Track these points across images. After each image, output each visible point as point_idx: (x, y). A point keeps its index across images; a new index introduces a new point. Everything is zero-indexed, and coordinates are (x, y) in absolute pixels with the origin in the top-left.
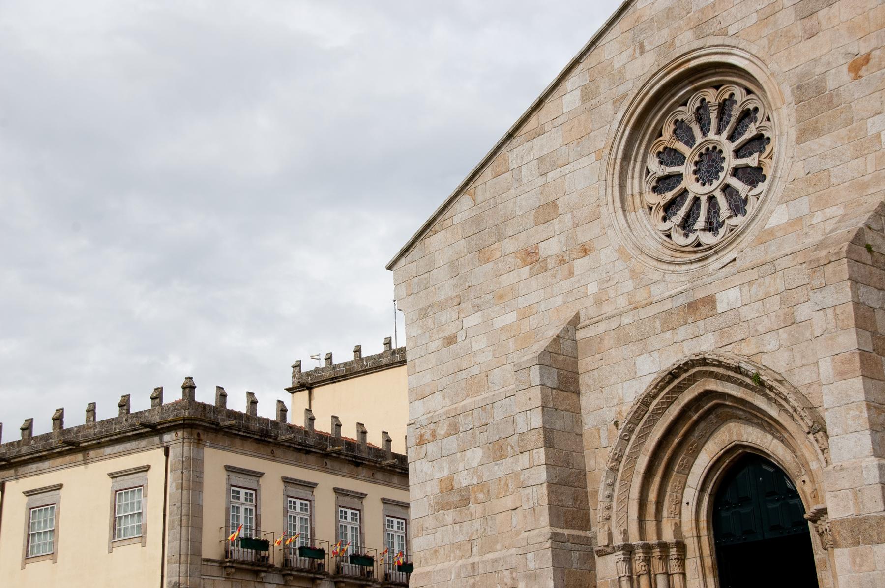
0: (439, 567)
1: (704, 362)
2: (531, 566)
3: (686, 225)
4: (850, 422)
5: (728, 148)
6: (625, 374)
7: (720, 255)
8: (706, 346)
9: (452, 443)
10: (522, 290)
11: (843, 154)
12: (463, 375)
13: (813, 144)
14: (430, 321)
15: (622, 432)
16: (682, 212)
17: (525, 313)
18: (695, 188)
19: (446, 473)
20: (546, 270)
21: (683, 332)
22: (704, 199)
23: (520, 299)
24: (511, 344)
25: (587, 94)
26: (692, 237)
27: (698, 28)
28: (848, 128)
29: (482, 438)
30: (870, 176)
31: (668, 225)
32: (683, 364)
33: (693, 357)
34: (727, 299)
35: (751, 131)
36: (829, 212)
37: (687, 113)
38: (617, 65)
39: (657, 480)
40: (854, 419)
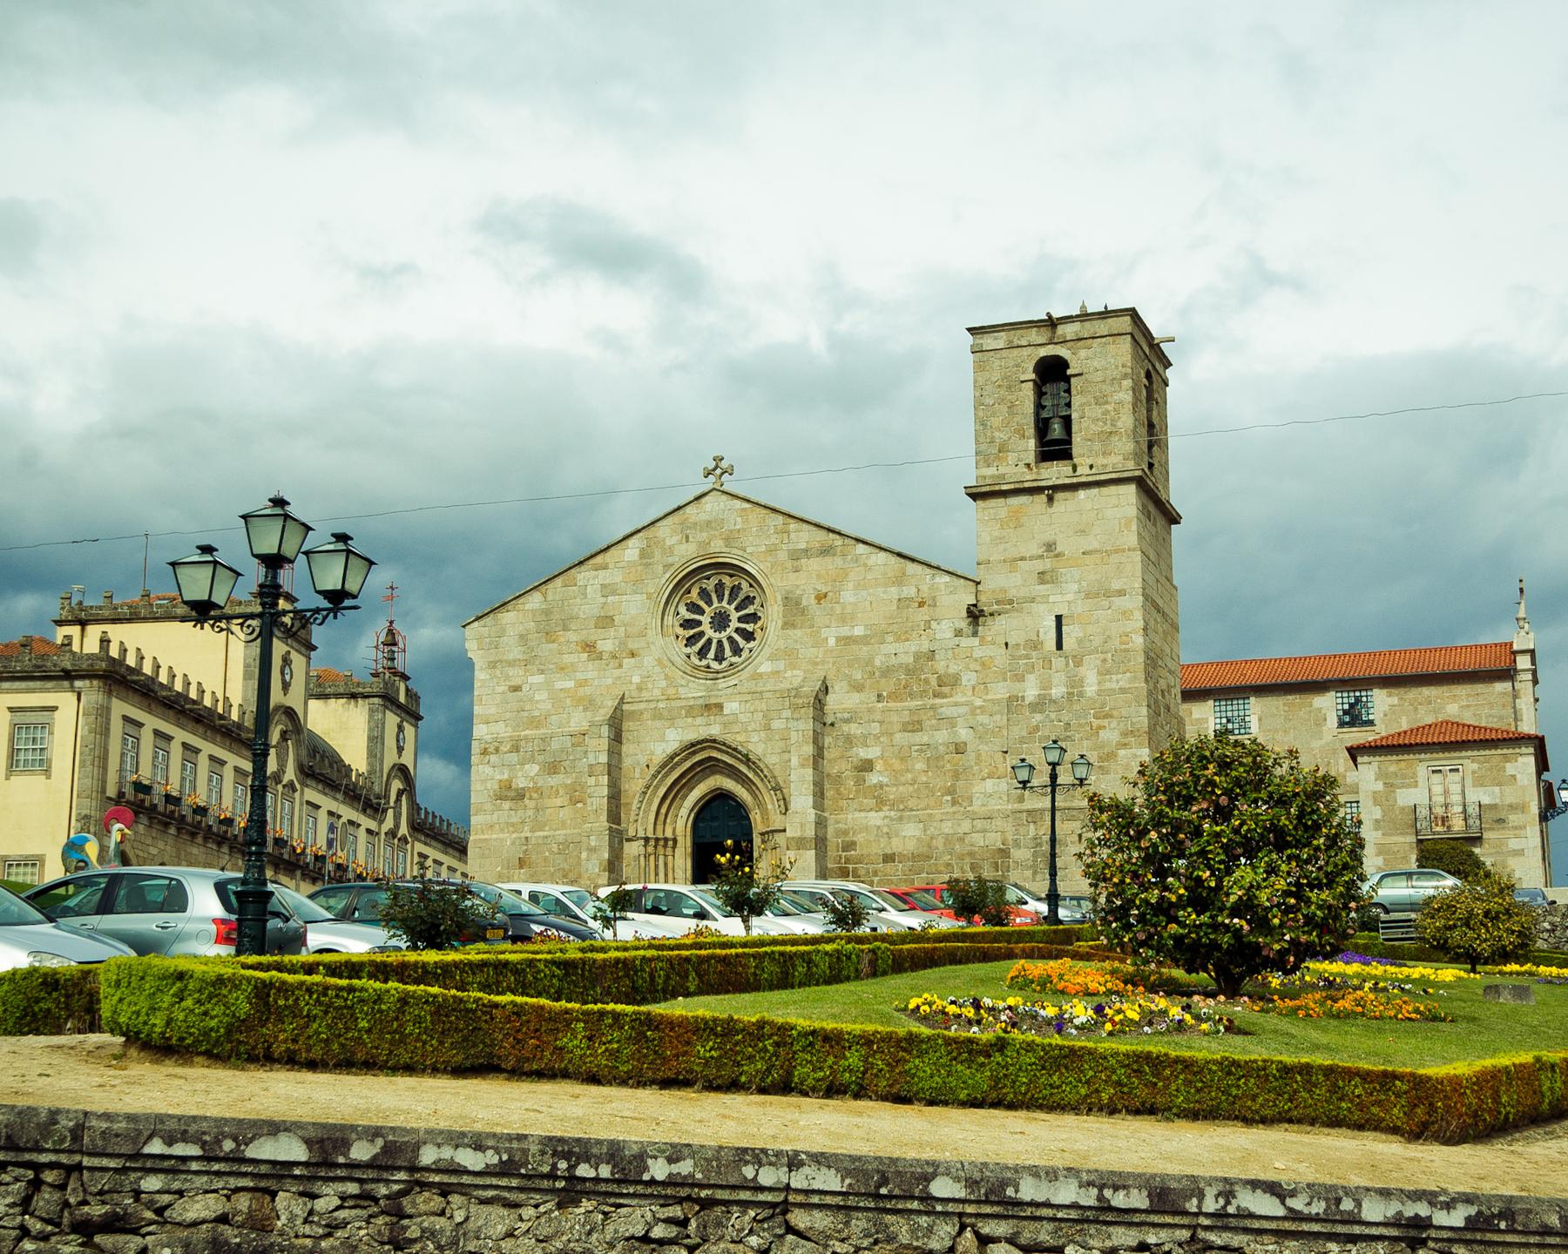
0: (494, 836)
1: (714, 741)
2: (593, 844)
3: (702, 653)
5: (734, 616)
8: (715, 731)
9: (514, 757)
12: (526, 714)
13: (790, 632)
14: (498, 672)
16: (700, 644)
17: (582, 683)
18: (710, 633)
19: (506, 776)
21: (699, 720)
22: (715, 641)
24: (568, 701)
25: (644, 554)
26: (704, 662)
27: (728, 541)
29: (541, 758)
31: (688, 650)
34: (731, 707)
35: (750, 610)
37: (710, 585)
38: (668, 543)
39: (668, 802)
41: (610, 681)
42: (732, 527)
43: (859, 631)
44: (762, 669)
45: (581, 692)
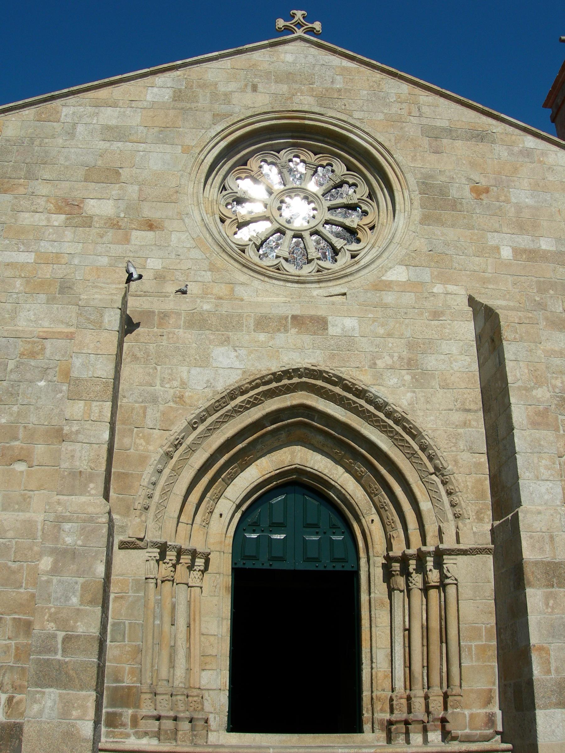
4: (542, 470)
6: (195, 359)
7: (322, 285)
10: (49, 235)
11: (465, 249)
13: (438, 230)
15: (194, 418)
20: (90, 227)
23: (42, 244)
24: (19, 284)
27: (321, 99)
28: (470, 231)
30: (491, 275)
32: (293, 369)
33: (309, 366)
36: (451, 288)
38: (222, 88)
40: (547, 468)
41: (104, 261)
42: (329, 85)
43: (546, 245)
44: (391, 276)
45: (46, 272)
